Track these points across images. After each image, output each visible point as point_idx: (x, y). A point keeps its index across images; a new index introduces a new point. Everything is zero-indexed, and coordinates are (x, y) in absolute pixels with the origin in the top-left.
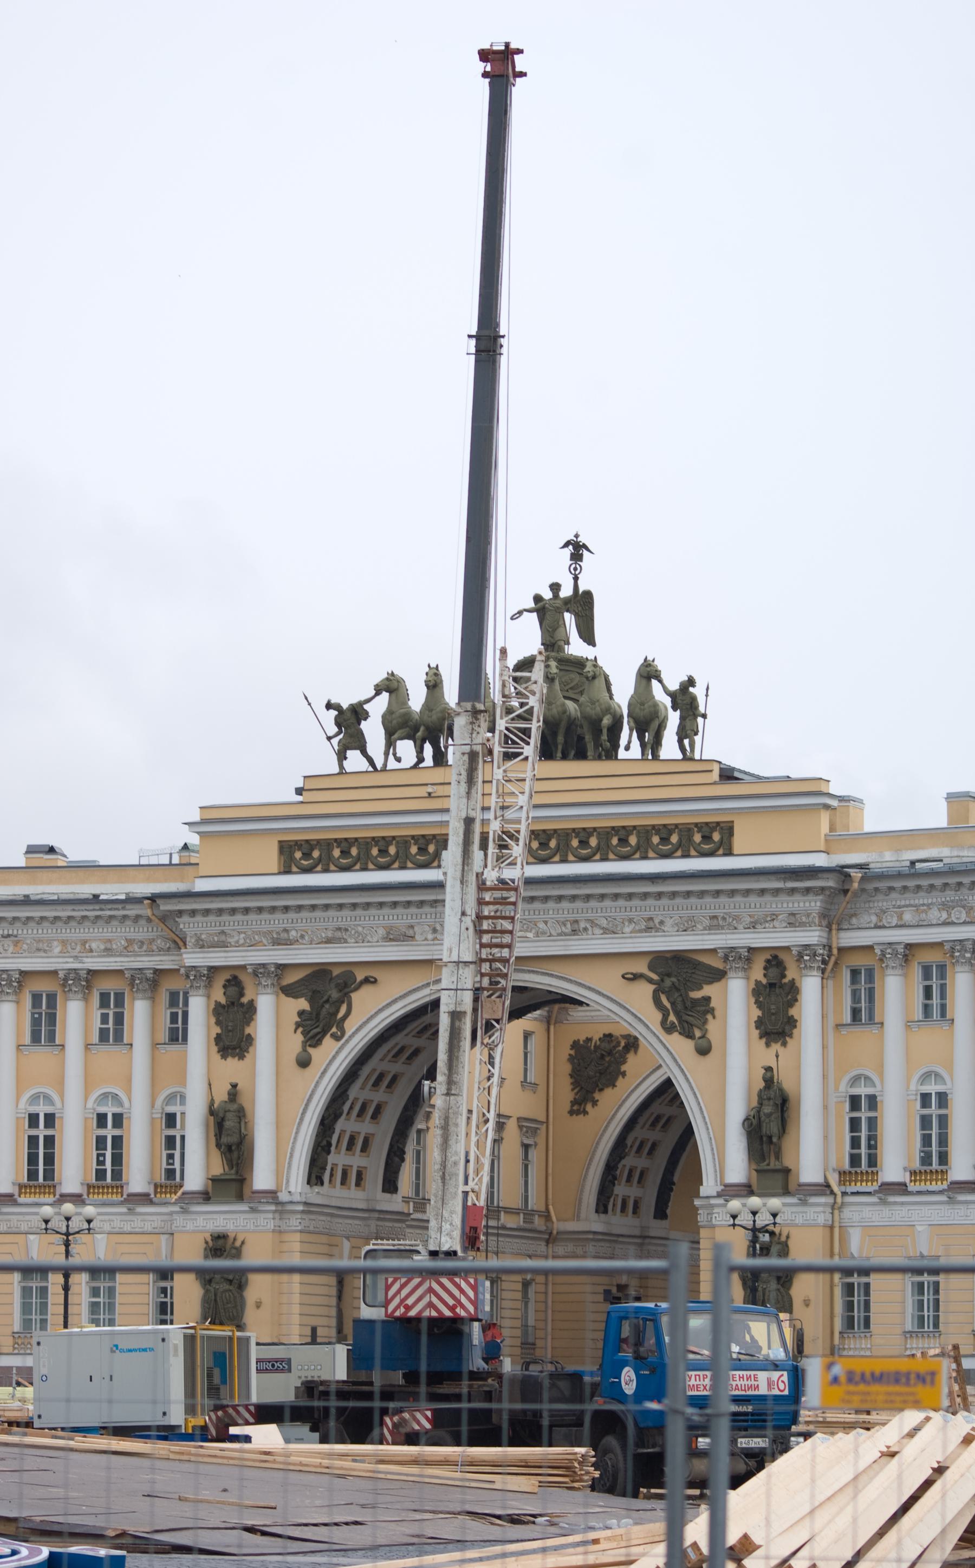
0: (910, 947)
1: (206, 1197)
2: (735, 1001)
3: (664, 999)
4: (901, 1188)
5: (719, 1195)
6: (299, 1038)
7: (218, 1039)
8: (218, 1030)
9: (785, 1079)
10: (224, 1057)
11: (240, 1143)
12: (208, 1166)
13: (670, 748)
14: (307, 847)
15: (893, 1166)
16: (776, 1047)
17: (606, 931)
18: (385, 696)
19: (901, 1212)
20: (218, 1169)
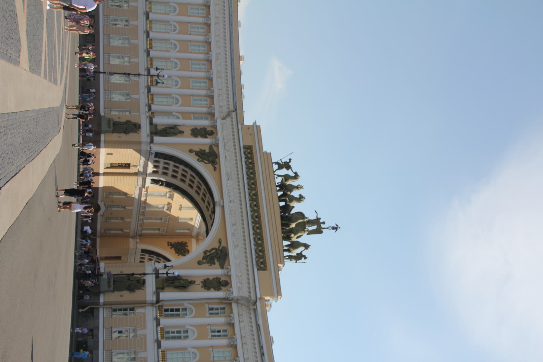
0: (233, 325)
1: (151, 123)
2: (214, 272)
3: (214, 251)
4: (158, 324)
5: (156, 268)
6: (198, 150)
7: (196, 128)
8: (199, 128)
9: (191, 287)
10: (191, 130)
11: (166, 133)
12: (160, 125)
13: (286, 254)
14: (251, 153)
15: (164, 322)
16: (201, 285)
17: (233, 233)
18: (293, 175)
19: (150, 324)
20: (159, 128)
